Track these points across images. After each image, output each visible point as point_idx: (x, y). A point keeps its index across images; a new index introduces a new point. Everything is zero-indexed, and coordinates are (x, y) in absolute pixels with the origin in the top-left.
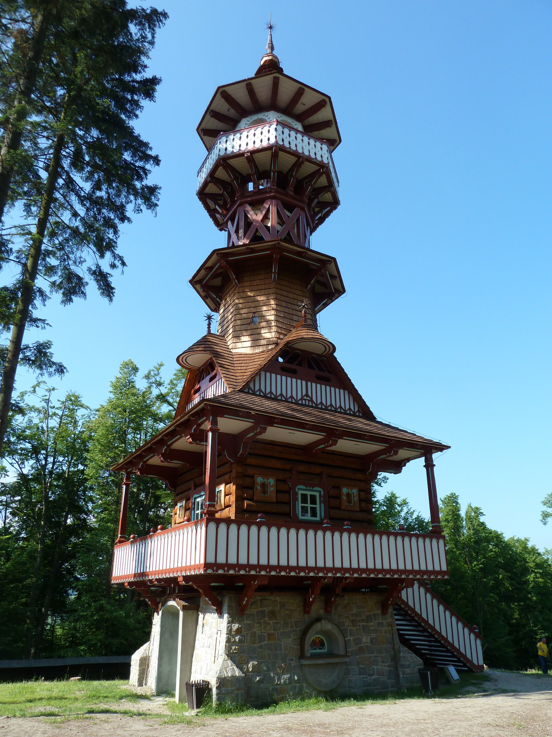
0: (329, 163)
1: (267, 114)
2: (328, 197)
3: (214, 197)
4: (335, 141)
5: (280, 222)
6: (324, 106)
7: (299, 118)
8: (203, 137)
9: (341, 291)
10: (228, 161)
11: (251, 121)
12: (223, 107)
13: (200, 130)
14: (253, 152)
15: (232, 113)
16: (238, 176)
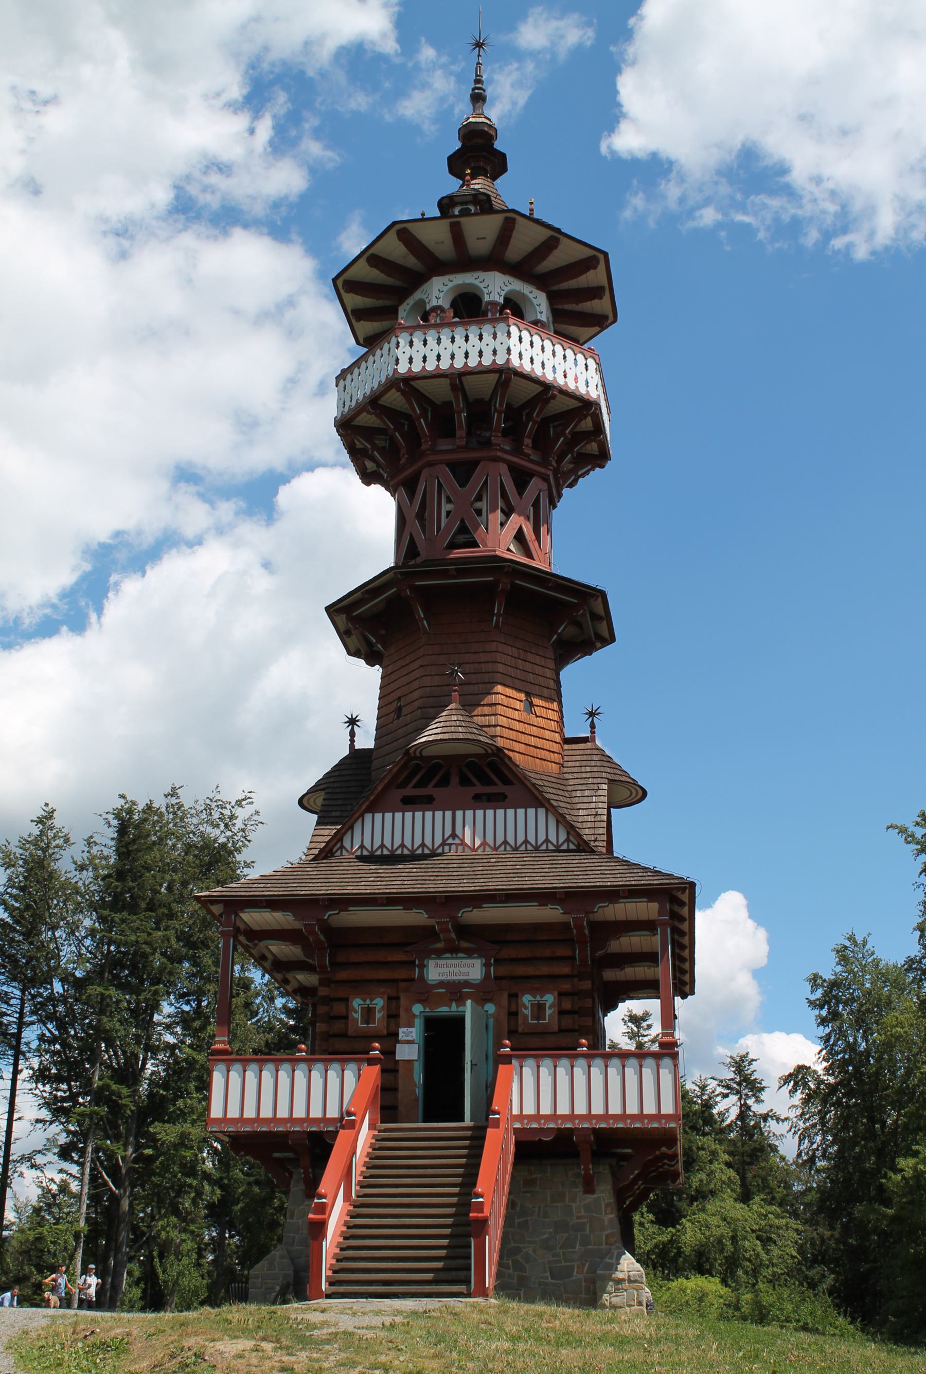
0: (599, 396)
1: (482, 275)
2: (593, 448)
3: (368, 433)
4: (606, 317)
5: (505, 508)
6: (595, 268)
7: (540, 281)
8: (344, 294)
9: (609, 638)
10: (412, 383)
11: (451, 285)
12: (395, 250)
13: (340, 283)
14: (466, 372)
15: (411, 262)
16: (427, 407)
